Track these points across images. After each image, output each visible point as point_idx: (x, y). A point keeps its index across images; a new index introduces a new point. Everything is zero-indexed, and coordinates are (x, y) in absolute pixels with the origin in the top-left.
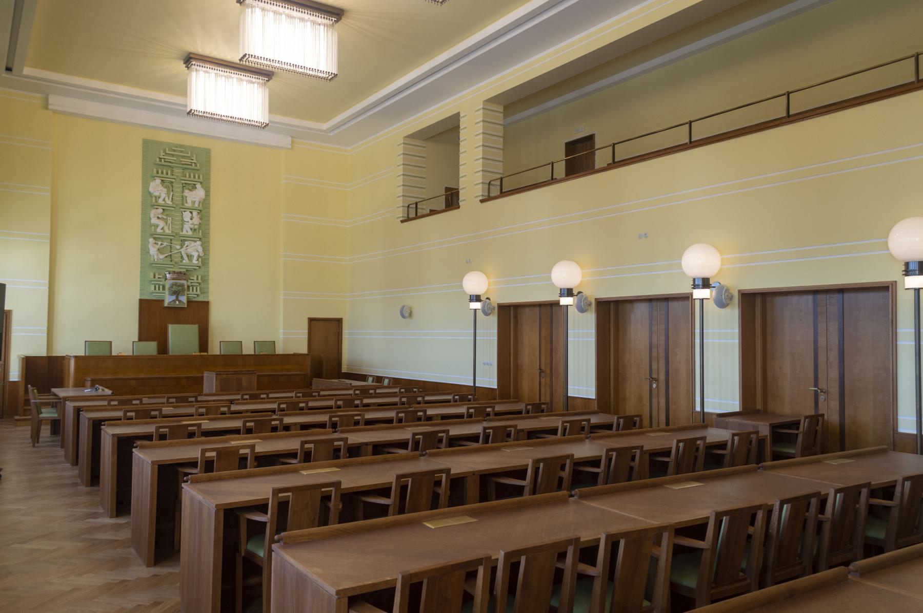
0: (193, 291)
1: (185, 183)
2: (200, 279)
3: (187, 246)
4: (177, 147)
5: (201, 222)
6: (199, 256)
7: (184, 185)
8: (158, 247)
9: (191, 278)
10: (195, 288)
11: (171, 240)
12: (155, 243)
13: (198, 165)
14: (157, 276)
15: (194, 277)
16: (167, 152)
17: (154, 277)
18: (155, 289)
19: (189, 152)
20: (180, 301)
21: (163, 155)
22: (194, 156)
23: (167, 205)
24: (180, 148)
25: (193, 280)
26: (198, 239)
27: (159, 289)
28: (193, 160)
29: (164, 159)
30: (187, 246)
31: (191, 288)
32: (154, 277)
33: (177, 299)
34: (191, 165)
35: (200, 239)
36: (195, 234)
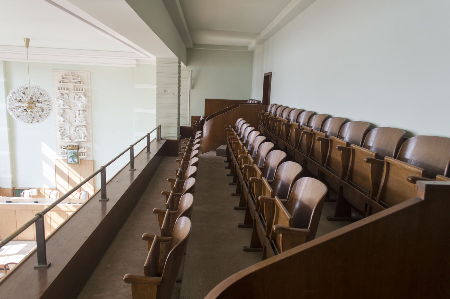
0: (82, 155)
1: (76, 94)
2: (86, 148)
3: (78, 130)
4: (69, 73)
5: (86, 116)
6: (85, 136)
7: (75, 95)
8: (62, 131)
9: (81, 148)
10: (83, 154)
11: (70, 127)
12: (61, 129)
13: (82, 82)
14: (63, 148)
15: (82, 147)
16: (64, 77)
17: (61, 148)
18: (62, 155)
19: (77, 76)
20: (74, 162)
21: (62, 79)
22: (80, 77)
23: (65, 108)
24: (72, 73)
25: (82, 149)
26: (84, 126)
27: (64, 155)
28: (79, 80)
29: (63, 81)
30: (78, 130)
31: (81, 154)
32: (61, 148)
33: (73, 160)
34: (77, 83)
35: (85, 127)
36: (82, 123)
